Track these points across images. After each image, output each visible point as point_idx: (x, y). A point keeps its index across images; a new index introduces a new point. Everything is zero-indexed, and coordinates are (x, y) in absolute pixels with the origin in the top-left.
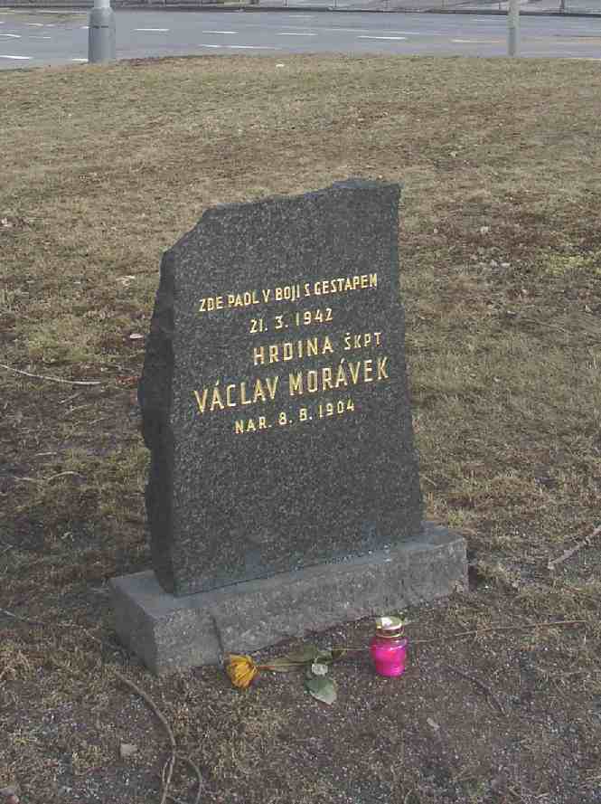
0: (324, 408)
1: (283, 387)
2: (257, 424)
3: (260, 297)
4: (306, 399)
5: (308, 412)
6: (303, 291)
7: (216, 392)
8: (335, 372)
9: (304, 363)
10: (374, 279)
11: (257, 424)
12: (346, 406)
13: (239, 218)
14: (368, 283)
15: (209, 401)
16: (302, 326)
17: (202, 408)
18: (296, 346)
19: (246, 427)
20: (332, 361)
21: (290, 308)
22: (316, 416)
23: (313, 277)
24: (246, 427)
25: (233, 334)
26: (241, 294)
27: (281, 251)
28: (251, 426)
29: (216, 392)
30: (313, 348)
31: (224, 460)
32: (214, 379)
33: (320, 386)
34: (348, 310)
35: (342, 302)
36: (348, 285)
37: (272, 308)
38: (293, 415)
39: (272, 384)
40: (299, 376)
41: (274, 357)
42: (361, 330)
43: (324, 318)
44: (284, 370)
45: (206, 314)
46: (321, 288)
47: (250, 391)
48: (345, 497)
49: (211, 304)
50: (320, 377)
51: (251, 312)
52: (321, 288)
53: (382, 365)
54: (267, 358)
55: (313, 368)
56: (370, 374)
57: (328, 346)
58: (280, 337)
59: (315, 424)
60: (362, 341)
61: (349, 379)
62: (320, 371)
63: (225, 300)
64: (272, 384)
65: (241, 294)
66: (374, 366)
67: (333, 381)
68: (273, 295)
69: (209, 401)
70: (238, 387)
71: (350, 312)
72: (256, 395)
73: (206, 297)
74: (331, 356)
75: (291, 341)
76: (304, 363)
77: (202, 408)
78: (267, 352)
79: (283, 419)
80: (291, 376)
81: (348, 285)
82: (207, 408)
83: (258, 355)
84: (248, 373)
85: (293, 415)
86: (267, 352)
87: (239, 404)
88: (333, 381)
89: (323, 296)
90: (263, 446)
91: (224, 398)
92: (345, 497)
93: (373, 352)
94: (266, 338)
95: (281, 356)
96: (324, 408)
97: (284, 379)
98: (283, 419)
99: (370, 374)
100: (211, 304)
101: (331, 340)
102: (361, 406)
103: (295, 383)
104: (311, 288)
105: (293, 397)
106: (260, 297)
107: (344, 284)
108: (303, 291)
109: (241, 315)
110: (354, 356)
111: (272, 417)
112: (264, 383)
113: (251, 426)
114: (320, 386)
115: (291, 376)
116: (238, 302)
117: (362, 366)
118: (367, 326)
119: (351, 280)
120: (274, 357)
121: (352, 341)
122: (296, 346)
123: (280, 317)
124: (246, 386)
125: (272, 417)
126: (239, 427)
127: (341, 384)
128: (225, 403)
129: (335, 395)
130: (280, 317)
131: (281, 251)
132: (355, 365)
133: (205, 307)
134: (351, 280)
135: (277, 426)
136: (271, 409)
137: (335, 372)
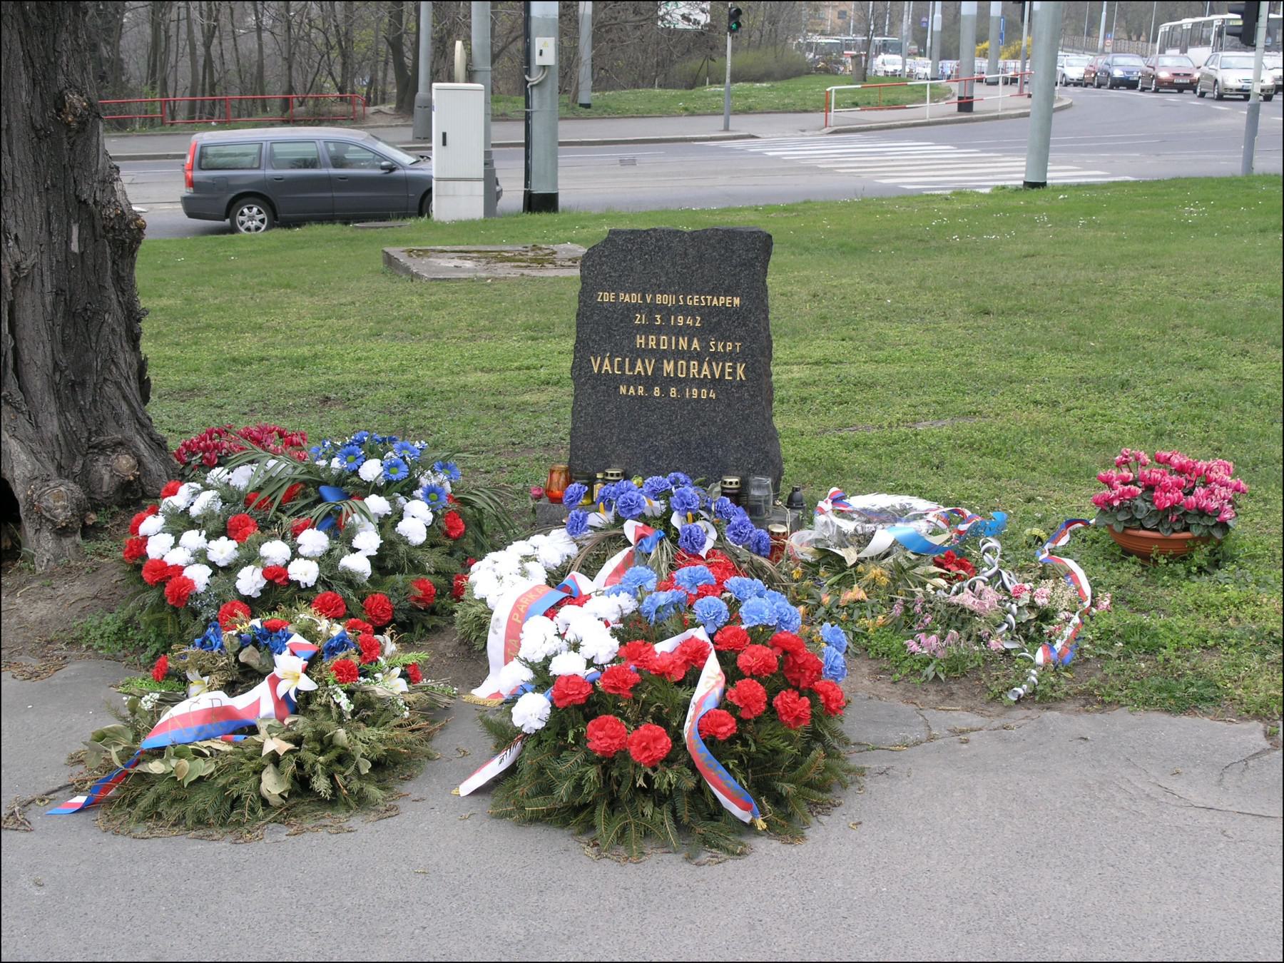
0: (690, 391)
1: (658, 369)
2: (636, 391)
3: (643, 298)
4: (676, 381)
5: (677, 391)
7: (607, 361)
8: (700, 366)
9: (677, 355)
10: (737, 301)
11: (636, 391)
12: (708, 394)
13: (630, 239)
14: (732, 303)
15: (601, 367)
16: (675, 326)
17: (596, 370)
18: (670, 340)
19: (628, 391)
20: (699, 357)
21: (667, 311)
22: (683, 396)
24: (628, 391)
25: (621, 321)
26: (630, 294)
27: (662, 267)
28: (632, 390)
29: (607, 361)
30: (683, 344)
31: (610, 411)
32: (605, 351)
33: (688, 373)
34: (715, 320)
35: (710, 313)
36: (715, 302)
37: (652, 309)
38: (665, 391)
39: (650, 364)
40: (672, 363)
41: (652, 344)
42: (725, 339)
43: (694, 323)
44: (660, 356)
45: (602, 303)
47: (632, 367)
48: (704, 464)
49: (607, 297)
50: (688, 368)
51: (637, 308)
53: (740, 371)
54: (647, 344)
55: (683, 359)
56: (730, 374)
57: (696, 344)
58: (658, 331)
59: (682, 402)
60: (724, 347)
61: (713, 374)
62: (688, 362)
63: (617, 296)
64: (650, 364)
65: (630, 294)
66: (734, 368)
67: (699, 372)
68: (654, 298)
69: (601, 367)
70: (624, 361)
71: (715, 323)
72: (637, 370)
73: (603, 292)
74: (698, 353)
75: (666, 335)
76: (677, 355)
77: (596, 370)
78: (647, 339)
79: (657, 391)
80: (665, 361)
81: (715, 302)
82: (600, 370)
83: (640, 341)
84: (631, 351)
85: (665, 391)
86: (647, 339)
87: (624, 373)
88: (699, 372)
89: (693, 307)
90: (640, 408)
91: (612, 366)
92: (704, 464)
93: (732, 357)
94: (648, 329)
95: (658, 344)
96: (690, 391)
97: (659, 362)
98: (657, 391)
99: (730, 374)
100: (607, 297)
101: (698, 340)
102: (720, 397)
103: (668, 367)
104: (685, 299)
105: (666, 378)
106: (643, 298)
107: (712, 301)
109: (628, 309)
110: (716, 357)
111: (648, 389)
112: (643, 362)
113: (632, 390)
114: (688, 373)
115: (665, 361)
116: (627, 299)
117: (723, 367)
118: (729, 336)
119: (718, 299)
120: (652, 344)
121: (716, 345)
122: (670, 340)
123: (658, 316)
124: (630, 361)
125: (648, 389)
126: (623, 390)
127: (705, 376)
128: (613, 370)
129: (701, 383)
130: (658, 316)
131: (662, 267)
132: (718, 365)
133: (602, 298)
134: (718, 299)
135: (651, 396)
136: (649, 382)
137: (700, 366)
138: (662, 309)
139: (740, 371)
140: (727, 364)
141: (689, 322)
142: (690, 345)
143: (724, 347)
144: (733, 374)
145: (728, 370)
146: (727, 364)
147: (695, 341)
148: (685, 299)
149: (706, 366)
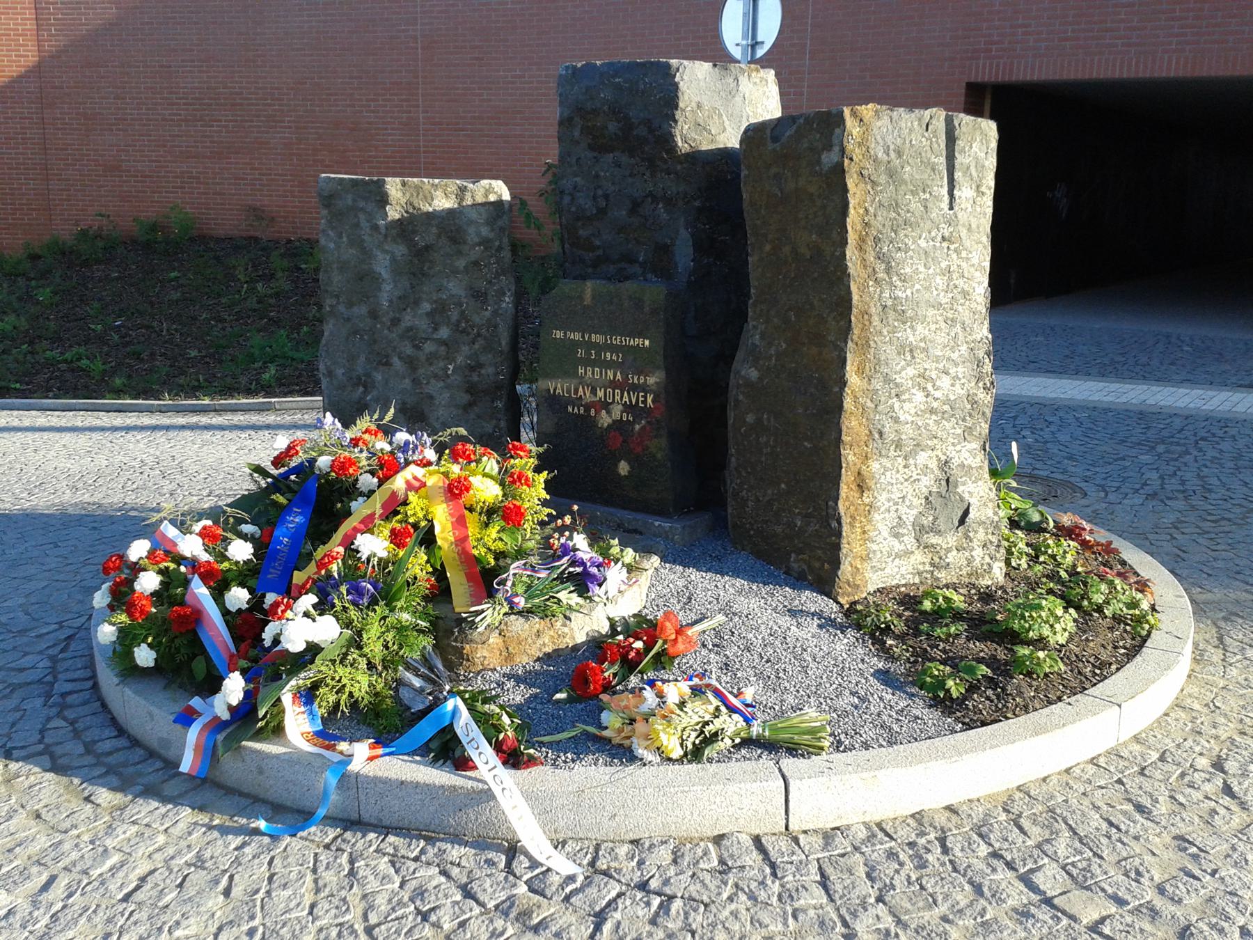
3: (583, 337)
6: (606, 340)
23: (613, 331)
37: (590, 345)
46: (617, 341)
52: (617, 341)
53: (649, 401)
57: (619, 376)
58: (593, 364)
61: (631, 401)
66: (645, 397)
67: (621, 400)
68: (590, 337)
81: (632, 342)
88: (621, 400)
104: (611, 339)
106: (583, 337)
108: (606, 340)
116: (572, 337)
121: (633, 378)
138: (596, 346)
139: (649, 401)
140: (641, 394)
141: (614, 358)
142: (615, 377)
143: (638, 379)
144: (645, 402)
145: (641, 399)
146: (641, 394)
147: (619, 374)
148: (611, 339)
149: (626, 394)
